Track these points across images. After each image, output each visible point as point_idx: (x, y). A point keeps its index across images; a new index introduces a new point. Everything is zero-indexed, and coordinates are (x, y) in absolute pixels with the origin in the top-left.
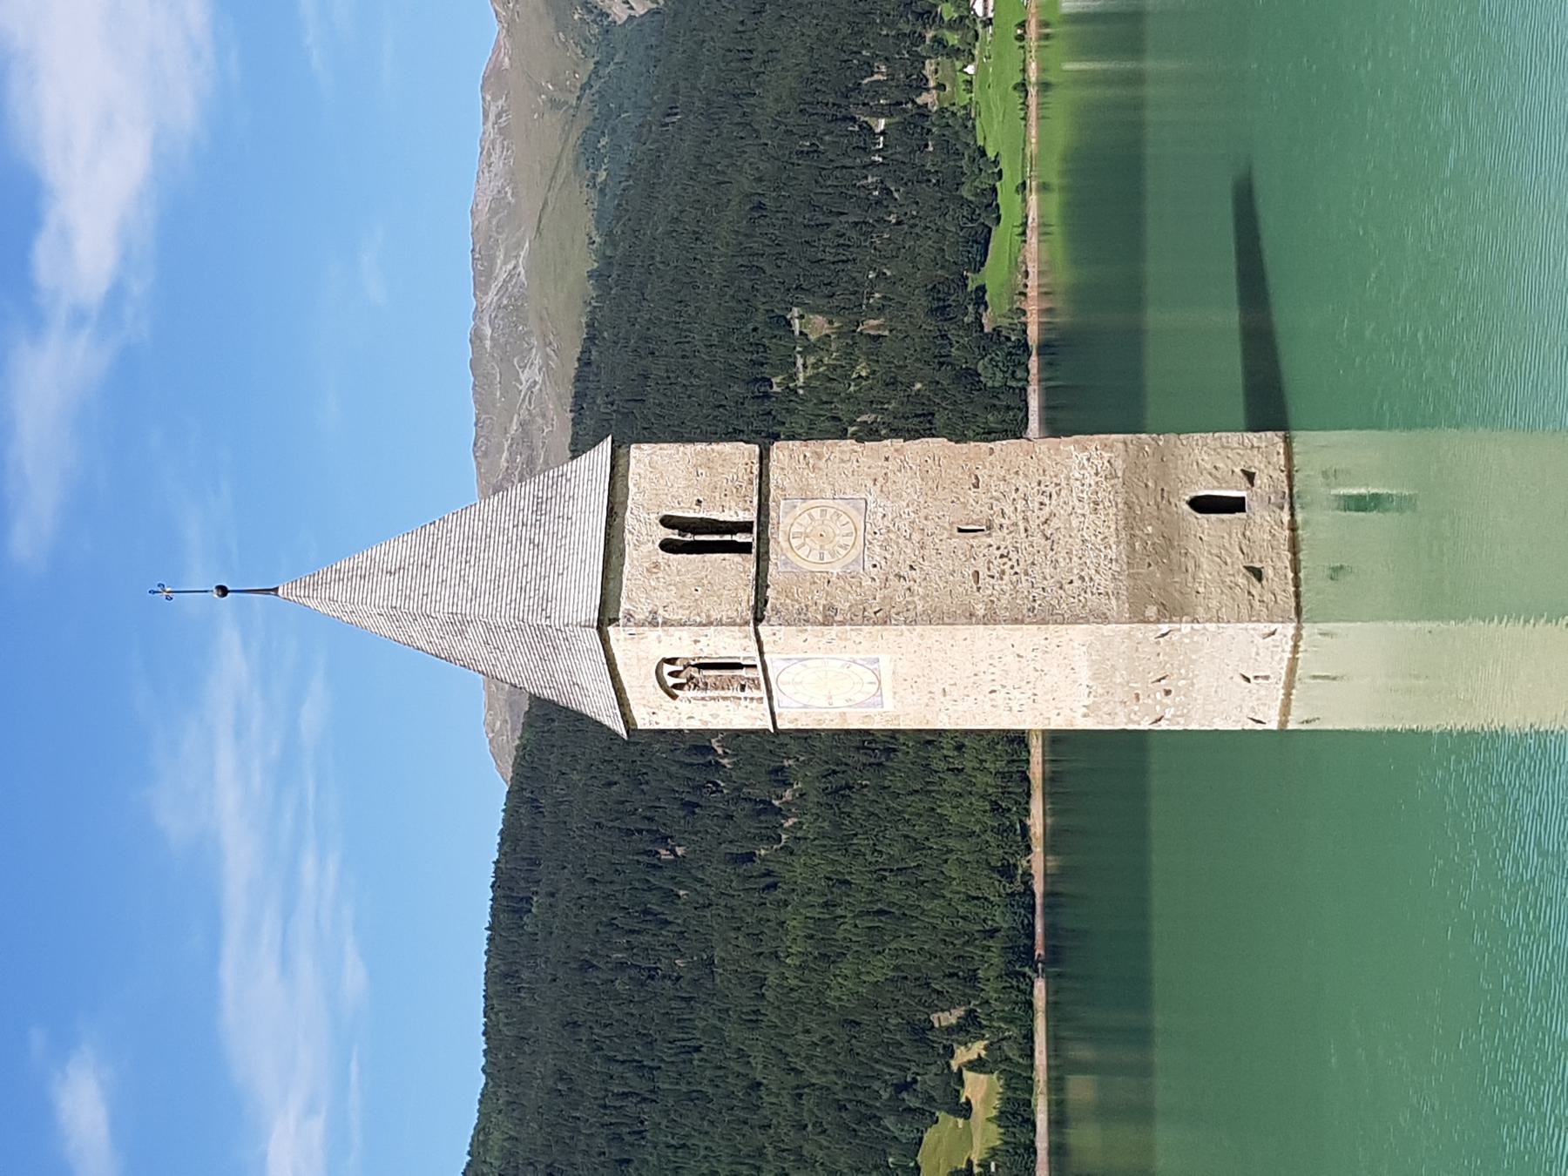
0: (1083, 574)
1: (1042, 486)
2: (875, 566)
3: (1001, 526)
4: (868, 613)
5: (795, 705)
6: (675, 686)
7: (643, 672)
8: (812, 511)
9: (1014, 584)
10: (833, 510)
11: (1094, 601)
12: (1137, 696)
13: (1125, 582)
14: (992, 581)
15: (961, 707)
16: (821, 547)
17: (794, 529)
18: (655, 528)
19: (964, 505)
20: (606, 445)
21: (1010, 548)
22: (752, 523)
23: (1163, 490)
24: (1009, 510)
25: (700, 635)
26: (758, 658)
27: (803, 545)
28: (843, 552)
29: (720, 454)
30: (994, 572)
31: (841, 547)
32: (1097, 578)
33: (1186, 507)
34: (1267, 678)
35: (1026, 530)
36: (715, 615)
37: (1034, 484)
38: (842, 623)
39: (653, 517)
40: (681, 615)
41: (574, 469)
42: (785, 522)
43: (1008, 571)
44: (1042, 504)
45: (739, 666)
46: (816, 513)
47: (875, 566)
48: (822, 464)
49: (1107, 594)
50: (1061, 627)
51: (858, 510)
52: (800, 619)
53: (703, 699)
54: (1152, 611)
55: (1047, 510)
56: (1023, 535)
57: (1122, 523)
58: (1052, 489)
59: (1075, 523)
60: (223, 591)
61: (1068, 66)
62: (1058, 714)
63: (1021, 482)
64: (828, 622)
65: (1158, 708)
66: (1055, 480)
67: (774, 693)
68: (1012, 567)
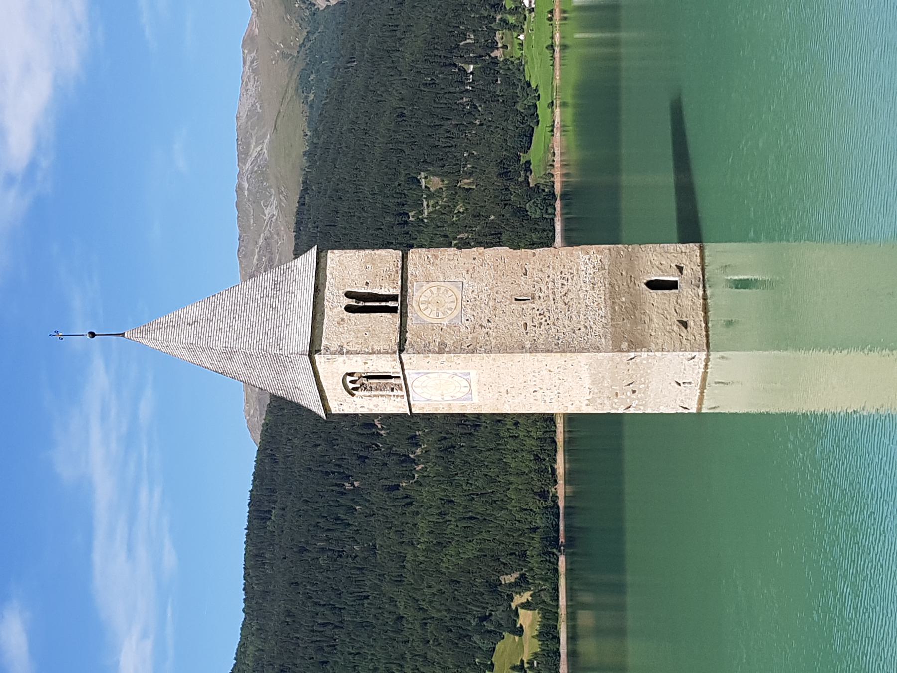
0: (586, 324)
1: (563, 274)
2: (468, 320)
3: (540, 297)
5: (423, 399)
6: (354, 389)
7: (335, 381)
8: (432, 288)
10: (444, 288)
11: (592, 339)
12: (617, 394)
14: (534, 328)
15: (517, 401)
16: (437, 309)
17: (422, 299)
18: (342, 298)
20: (314, 250)
21: (545, 309)
22: (398, 295)
23: (631, 276)
25: (367, 360)
26: (401, 373)
27: (427, 308)
28: (451, 312)
29: (380, 255)
30: (536, 323)
31: (449, 309)
32: (594, 326)
33: (645, 286)
34: (690, 383)
35: (554, 299)
36: (376, 348)
37: (558, 273)
38: (449, 353)
39: (342, 293)
40: (357, 348)
41: (295, 264)
42: (416, 294)
43: (544, 323)
44: (562, 284)
45: (390, 377)
46: (434, 290)
47: (468, 320)
48: (437, 262)
49: (600, 336)
50: (573, 354)
51: (458, 287)
52: (425, 350)
53: (369, 396)
54: (625, 346)
55: (565, 288)
56: (553, 302)
57: (608, 295)
58: (566, 276)
59: (581, 296)
60: (93, 335)
61: (577, 36)
62: (572, 404)
63: (550, 271)
64: (440, 352)
65: (629, 400)
66: (570, 271)
67: (410, 393)
68: (546, 320)
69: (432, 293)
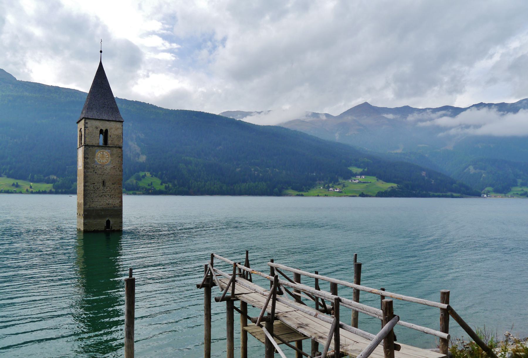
3: (104, 188)
4: (86, 165)
9: (92, 190)
11: (88, 204)
13: (92, 209)
16: (100, 157)
17: (104, 153)
19: (109, 182)
24: (107, 189)
28: (99, 161)
29: (121, 140)
33: (107, 219)
35: (103, 192)
36: (86, 138)
37: (112, 194)
38: (84, 160)
42: (106, 151)
43: (95, 189)
44: (109, 195)
46: (108, 156)
53: (80, 136)
54: (86, 213)
58: (112, 197)
60: (101, 52)
68: (96, 190)
69: (106, 156)
